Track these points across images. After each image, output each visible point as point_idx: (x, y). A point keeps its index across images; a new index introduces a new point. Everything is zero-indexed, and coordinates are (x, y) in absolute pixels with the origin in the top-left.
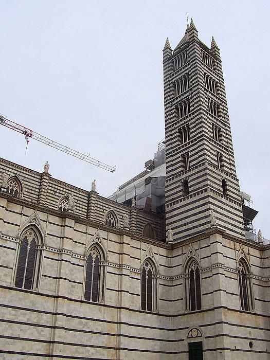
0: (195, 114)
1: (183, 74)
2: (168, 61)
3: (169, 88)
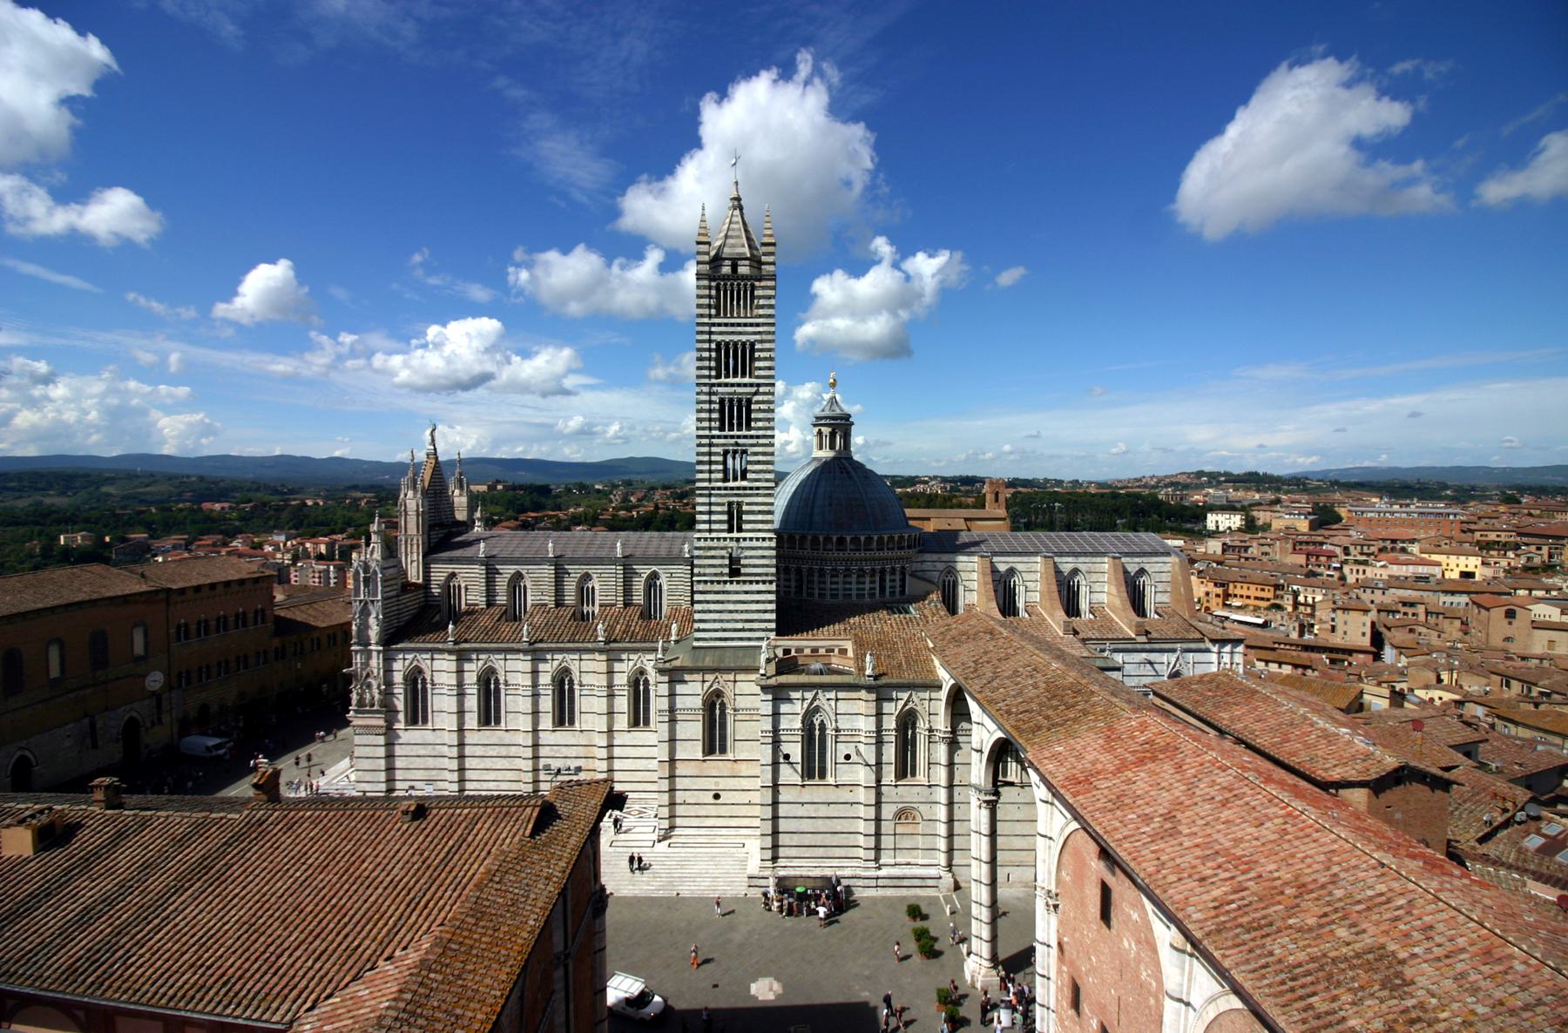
0: (761, 441)
1: (744, 338)
3: (710, 350)
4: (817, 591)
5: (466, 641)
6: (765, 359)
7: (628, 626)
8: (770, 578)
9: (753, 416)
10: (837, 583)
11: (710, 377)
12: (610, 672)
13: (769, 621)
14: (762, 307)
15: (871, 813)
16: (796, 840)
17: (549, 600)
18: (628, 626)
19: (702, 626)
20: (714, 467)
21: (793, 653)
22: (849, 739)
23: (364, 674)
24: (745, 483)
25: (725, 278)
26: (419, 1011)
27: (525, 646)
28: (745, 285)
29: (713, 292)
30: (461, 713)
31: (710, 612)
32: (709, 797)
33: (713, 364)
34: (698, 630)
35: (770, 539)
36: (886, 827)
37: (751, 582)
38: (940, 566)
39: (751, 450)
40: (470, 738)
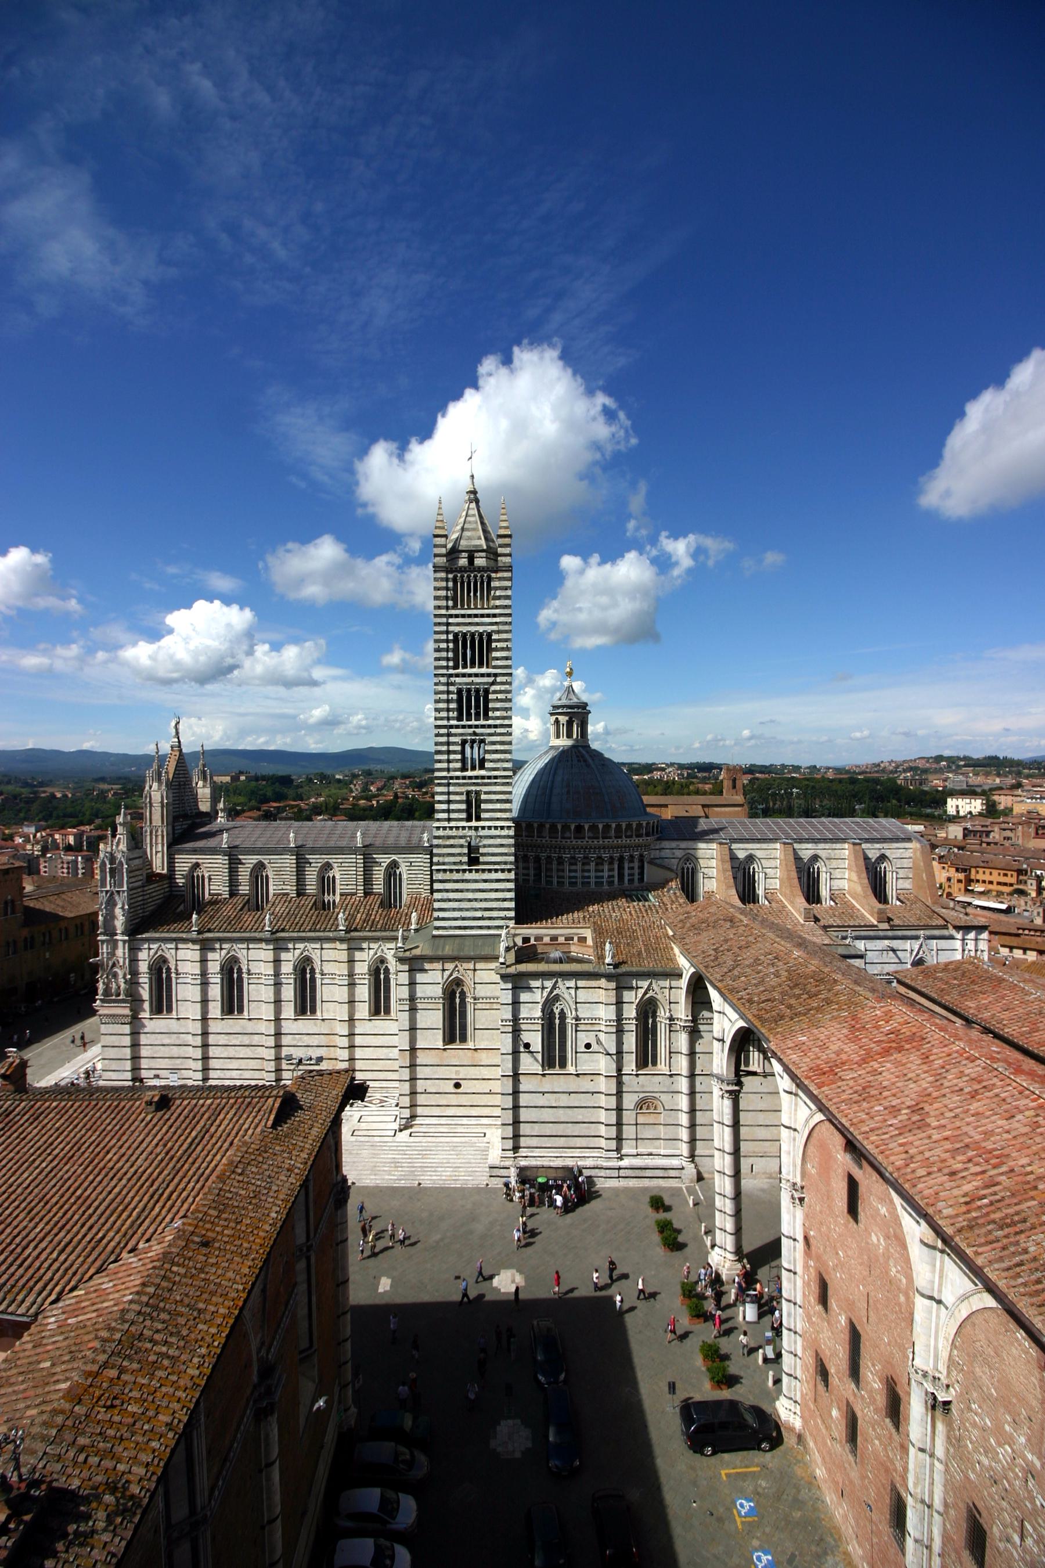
0: (499, 730)
1: (481, 629)
2: (447, 572)
3: (447, 641)
4: (555, 880)
5: (209, 931)
6: (502, 649)
7: (369, 915)
8: (508, 867)
9: (491, 705)
10: (576, 871)
11: (447, 667)
12: (351, 961)
13: (508, 909)
14: (499, 598)
15: (612, 1102)
16: (537, 1129)
17: (291, 889)
18: (369, 915)
19: (442, 914)
20: (452, 757)
21: (532, 942)
22: (589, 1027)
23: (111, 963)
24: (483, 773)
25: (462, 570)
26: (162, 1305)
27: (268, 935)
28: (482, 577)
29: (451, 584)
30: (205, 1001)
31: (450, 900)
32: (449, 1087)
33: (451, 655)
34: (438, 919)
35: (509, 828)
36: (628, 1117)
37: (490, 871)
38: (679, 854)
39: (489, 739)
40: (213, 1027)
